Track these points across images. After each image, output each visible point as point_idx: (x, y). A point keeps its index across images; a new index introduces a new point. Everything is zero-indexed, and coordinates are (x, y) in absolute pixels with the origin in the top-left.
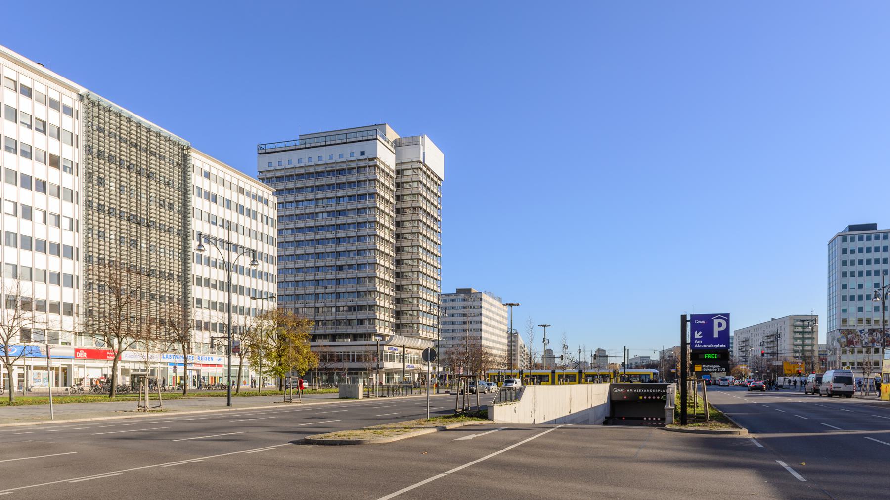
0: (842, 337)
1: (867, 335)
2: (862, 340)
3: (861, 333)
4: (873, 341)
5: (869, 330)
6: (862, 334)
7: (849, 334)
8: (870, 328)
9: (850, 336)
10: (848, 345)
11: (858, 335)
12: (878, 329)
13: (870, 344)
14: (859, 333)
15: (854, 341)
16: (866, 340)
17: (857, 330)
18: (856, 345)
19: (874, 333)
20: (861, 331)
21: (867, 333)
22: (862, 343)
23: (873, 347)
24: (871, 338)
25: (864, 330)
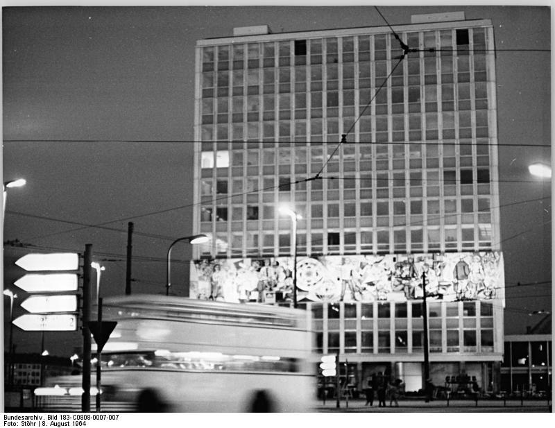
0: (200, 278)
3: (238, 267)
10: (211, 297)
13: (255, 296)
19: (263, 269)
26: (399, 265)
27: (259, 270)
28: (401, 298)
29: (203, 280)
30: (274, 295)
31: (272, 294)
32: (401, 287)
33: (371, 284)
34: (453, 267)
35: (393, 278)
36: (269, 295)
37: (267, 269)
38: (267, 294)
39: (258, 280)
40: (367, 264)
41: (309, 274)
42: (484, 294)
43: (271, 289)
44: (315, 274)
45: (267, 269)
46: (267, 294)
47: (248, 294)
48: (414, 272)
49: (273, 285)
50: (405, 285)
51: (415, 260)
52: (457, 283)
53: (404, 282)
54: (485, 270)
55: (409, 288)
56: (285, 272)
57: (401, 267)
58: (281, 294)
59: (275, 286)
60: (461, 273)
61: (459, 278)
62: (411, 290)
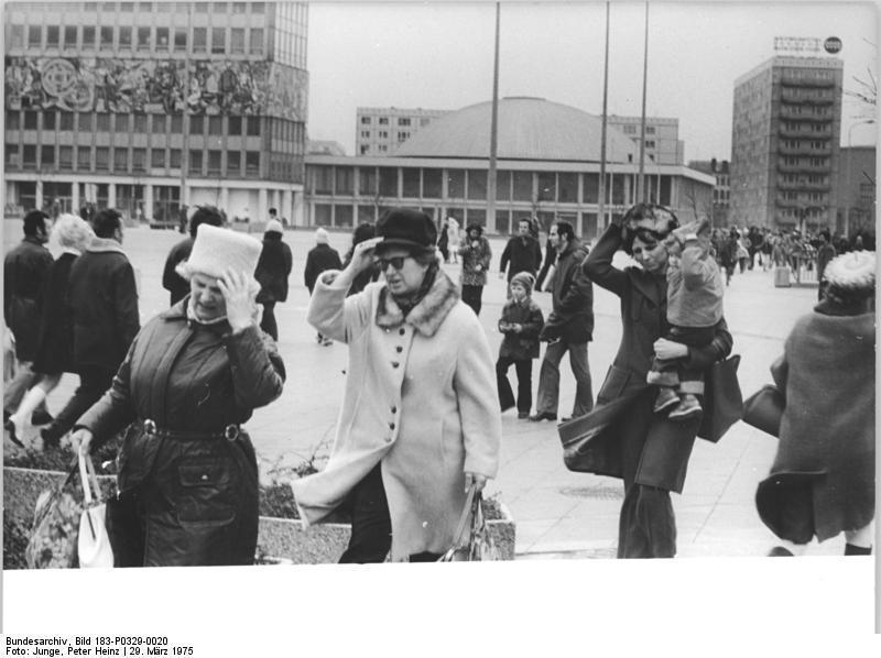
28: (159, 108)
30: (20, 101)
32: (159, 98)
33: (127, 92)
34: (218, 76)
35: (152, 86)
43: (17, 94)
44: (65, 79)
45: (13, 70)
49: (19, 86)
50: (164, 95)
53: (164, 91)
54: (254, 82)
55: (169, 99)
56: (33, 73)
57: (162, 74)
58: (28, 99)
59: (22, 90)
60: (226, 84)
62: (171, 103)
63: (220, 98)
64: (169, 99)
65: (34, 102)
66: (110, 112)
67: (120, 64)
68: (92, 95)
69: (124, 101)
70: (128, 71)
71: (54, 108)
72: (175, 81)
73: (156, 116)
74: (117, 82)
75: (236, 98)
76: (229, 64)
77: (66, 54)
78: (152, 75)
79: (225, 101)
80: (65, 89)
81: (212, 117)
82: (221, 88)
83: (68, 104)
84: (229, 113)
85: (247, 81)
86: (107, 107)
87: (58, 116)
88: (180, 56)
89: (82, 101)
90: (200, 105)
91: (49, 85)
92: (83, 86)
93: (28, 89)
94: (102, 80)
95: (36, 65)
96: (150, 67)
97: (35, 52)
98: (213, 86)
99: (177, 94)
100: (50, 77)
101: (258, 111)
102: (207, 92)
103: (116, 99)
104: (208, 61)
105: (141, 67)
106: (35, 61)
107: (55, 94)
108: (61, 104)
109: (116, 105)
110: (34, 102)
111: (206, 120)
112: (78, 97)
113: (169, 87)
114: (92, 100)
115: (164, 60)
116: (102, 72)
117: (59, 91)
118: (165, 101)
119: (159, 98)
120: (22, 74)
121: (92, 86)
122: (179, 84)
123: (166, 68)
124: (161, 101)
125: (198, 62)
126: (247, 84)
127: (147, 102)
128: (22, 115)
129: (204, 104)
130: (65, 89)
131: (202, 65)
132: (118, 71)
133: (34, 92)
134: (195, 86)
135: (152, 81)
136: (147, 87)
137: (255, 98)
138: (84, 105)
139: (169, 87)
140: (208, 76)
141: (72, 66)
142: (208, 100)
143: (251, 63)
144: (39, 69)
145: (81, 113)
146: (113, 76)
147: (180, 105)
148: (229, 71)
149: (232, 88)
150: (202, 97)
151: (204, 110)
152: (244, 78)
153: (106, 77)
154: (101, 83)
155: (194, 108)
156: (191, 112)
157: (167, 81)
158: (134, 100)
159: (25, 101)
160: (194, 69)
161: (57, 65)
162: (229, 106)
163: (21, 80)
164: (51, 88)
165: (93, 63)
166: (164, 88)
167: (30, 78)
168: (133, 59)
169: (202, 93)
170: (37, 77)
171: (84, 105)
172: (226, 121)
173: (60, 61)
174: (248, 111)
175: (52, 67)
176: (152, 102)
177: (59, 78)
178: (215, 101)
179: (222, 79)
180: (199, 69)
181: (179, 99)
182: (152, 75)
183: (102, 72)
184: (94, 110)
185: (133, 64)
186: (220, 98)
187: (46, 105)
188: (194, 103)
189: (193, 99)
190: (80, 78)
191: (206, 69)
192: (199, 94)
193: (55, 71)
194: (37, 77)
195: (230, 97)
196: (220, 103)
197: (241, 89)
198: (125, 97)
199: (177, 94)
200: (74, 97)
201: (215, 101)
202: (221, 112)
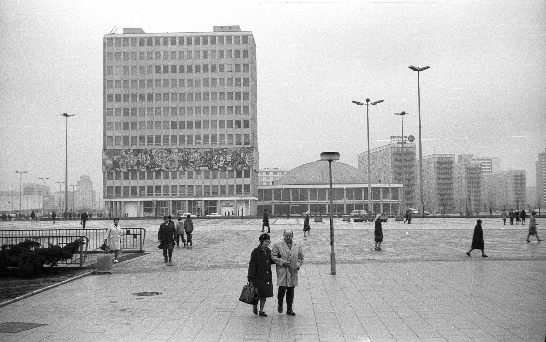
0: (108, 159)
1: (132, 156)
2: (127, 163)
3: (127, 154)
4: (138, 163)
5: (134, 150)
6: (127, 156)
7: (115, 155)
8: (135, 148)
9: (115, 157)
10: (113, 168)
11: (123, 157)
12: (142, 150)
13: (135, 168)
14: (124, 154)
15: (120, 163)
16: (132, 162)
17: (122, 151)
18: (122, 168)
19: (140, 155)
20: (126, 152)
21: (132, 154)
22: (128, 166)
23: (138, 171)
24: (136, 159)
25: (129, 150)
26: (206, 153)
27: (138, 155)
29: (109, 160)
30: (145, 167)
31: (144, 167)
33: (192, 162)
36: (143, 167)
37: (141, 155)
38: (142, 167)
39: (137, 160)
40: (191, 152)
41: (162, 157)
42: (246, 167)
43: (143, 165)
46: (142, 167)
47: (132, 167)
48: (213, 157)
49: (145, 162)
51: (214, 151)
52: (233, 162)
53: (208, 161)
54: (247, 156)
55: (211, 165)
57: (207, 154)
58: (149, 167)
59: (146, 163)
60: (235, 157)
61: (234, 160)
62: (212, 165)
63: (232, 163)
64: (211, 165)
65: (152, 168)
66: (185, 170)
67: (189, 150)
68: (177, 164)
69: (192, 166)
70: (193, 153)
71: (161, 170)
72: (213, 157)
73: (205, 171)
74: (187, 158)
75: (239, 163)
76: (236, 149)
77: (165, 147)
78: (203, 155)
79: (234, 165)
80: (165, 162)
81: (229, 171)
82: (233, 159)
83: (166, 168)
84: (236, 169)
85: (244, 156)
86: (184, 169)
87: (162, 173)
88: (215, 147)
89: (172, 167)
90: (224, 166)
91: (158, 161)
92: (173, 160)
93: (148, 162)
94: (181, 158)
95: (151, 152)
96: (202, 151)
97: (150, 147)
98: (229, 158)
99: (214, 162)
100: (158, 158)
101: (249, 168)
102: (227, 161)
103: (187, 166)
104: (226, 148)
105: (198, 152)
106: (151, 151)
107: (161, 164)
108: (164, 168)
109: (187, 167)
110: (152, 168)
111: (227, 172)
112: (171, 165)
113: (210, 160)
114: (177, 166)
115: (208, 149)
116: (181, 154)
117: (162, 163)
118: (209, 166)
119: (206, 164)
120: (145, 156)
121: (177, 160)
122: (214, 158)
123: (209, 151)
124: (207, 166)
125: (222, 149)
126: (244, 157)
127: (201, 166)
128: (146, 173)
129: (226, 166)
130: (165, 162)
131: (224, 150)
132: (189, 153)
133: (151, 164)
134: (221, 158)
135: (203, 157)
136: (201, 160)
137: (247, 163)
138: (174, 168)
139: (210, 160)
140: (227, 155)
141: (167, 152)
142: (227, 164)
143: (245, 148)
144: (153, 154)
145: (172, 172)
146: (186, 156)
147: (215, 167)
148: (236, 152)
149: (237, 159)
150: (224, 163)
151: (225, 168)
152: (242, 155)
153: (183, 156)
154: (181, 159)
155: (221, 168)
156: (220, 169)
157: (210, 157)
158: (195, 166)
159: (147, 168)
160: (220, 152)
161: (161, 152)
162: (236, 166)
163: (145, 159)
164: (159, 162)
165: (177, 151)
166: (208, 160)
167: (149, 158)
168: (194, 149)
169: (225, 161)
170: (153, 158)
171: (174, 168)
172: (235, 172)
173: (163, 150)
174: (245, 168)
175: (158, 153)
176: (203, 166)
177: (162, 157)
178: (230, 164)
179: (233, 156)
180: (223, 151)
181: (215, 164)
182: (203, 155)
183: (181, 154)
184: (178, 170)
185: (196, 150)
186: (232, 163)
187: (157, 169)
188: (221, 166)
189: (221, 164)
190: (171, 157)
191: (226, 151)
192: (223, 162)
193: (160, 155)
194: (153, 158)
195: (237, 162)
196: (232, 165)
197: (241, 159)
198: (191, 164)
199: (214, 162)
200: (169, 165)
201: (230, 164)
202: (233, 169)
